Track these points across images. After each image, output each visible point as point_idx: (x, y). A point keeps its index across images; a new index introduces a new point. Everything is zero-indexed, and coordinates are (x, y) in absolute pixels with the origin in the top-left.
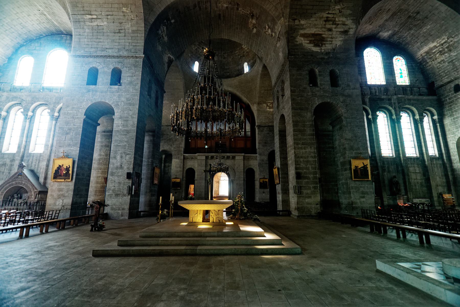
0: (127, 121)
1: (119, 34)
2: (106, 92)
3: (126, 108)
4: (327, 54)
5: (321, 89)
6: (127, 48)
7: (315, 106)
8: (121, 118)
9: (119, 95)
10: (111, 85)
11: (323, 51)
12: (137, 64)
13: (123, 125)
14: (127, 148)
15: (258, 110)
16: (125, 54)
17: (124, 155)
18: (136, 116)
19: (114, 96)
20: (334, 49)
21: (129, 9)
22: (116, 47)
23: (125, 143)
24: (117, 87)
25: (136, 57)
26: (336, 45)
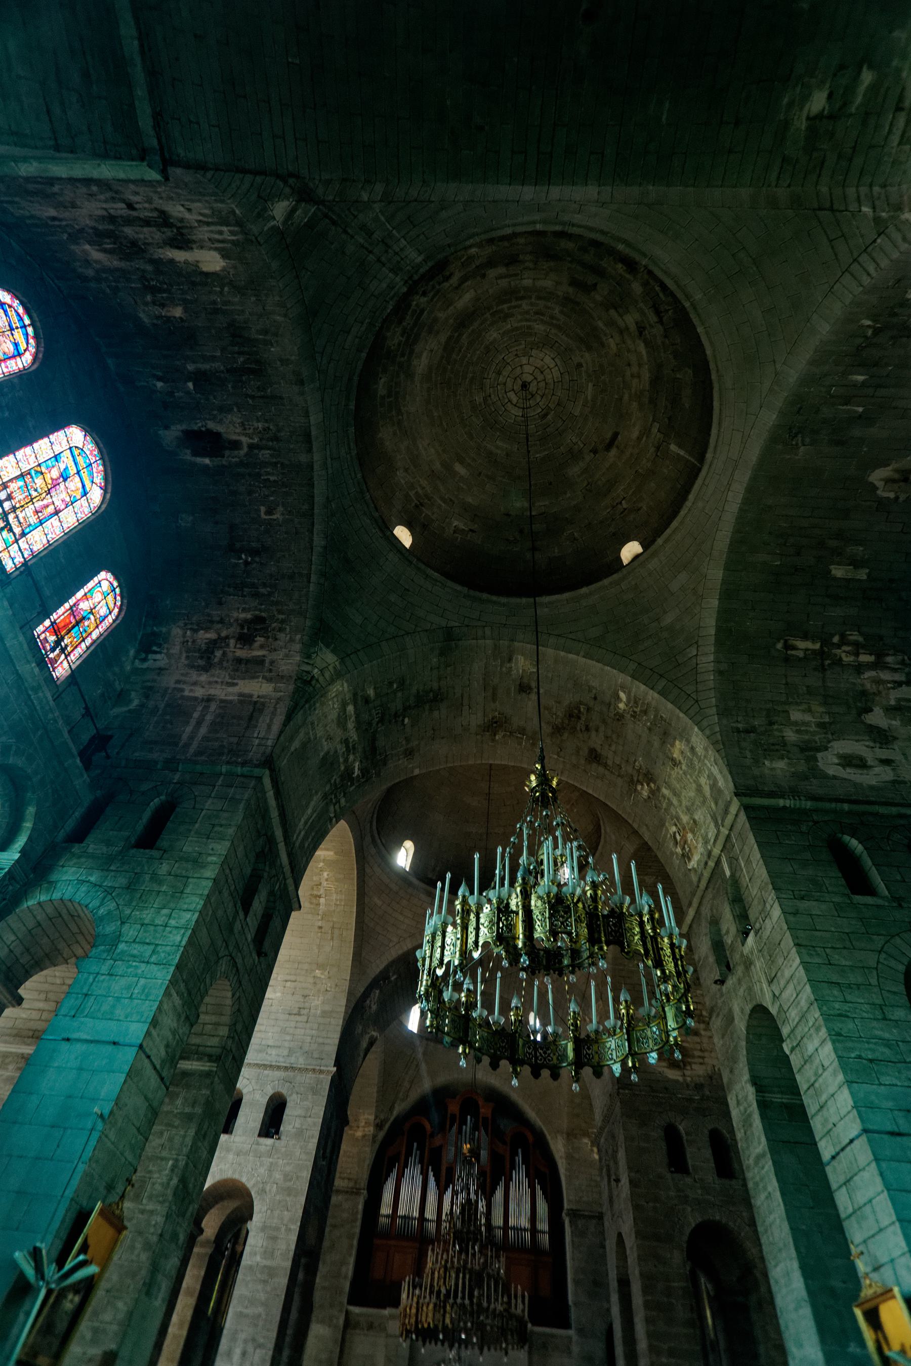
0: (274, 1239)
1: (298, 1018)
2: (247, 1153)
3: (280, 1202)
4: (699, 1087)
5: (695, 1181)
6: (306, 1047)
7: (688, 1231)
8: (264, 1228)
9: (271, 1163)
10: (260, 1135)
11: (689, 1079)
12: (319, 1086)
13: (265, 1252)
14: (261, 1323)
15: (569, 1157)
16: (301, 1062)
17: (250, 1349)
18: (296, 1227)
19: (262, 1165)
20: (711, 1078)
21: (326, 973)
22: (286, 1044)
23: (260, 1310)
24: (269, 1141)
25: (321, 1072)
26: (714, 1066)
